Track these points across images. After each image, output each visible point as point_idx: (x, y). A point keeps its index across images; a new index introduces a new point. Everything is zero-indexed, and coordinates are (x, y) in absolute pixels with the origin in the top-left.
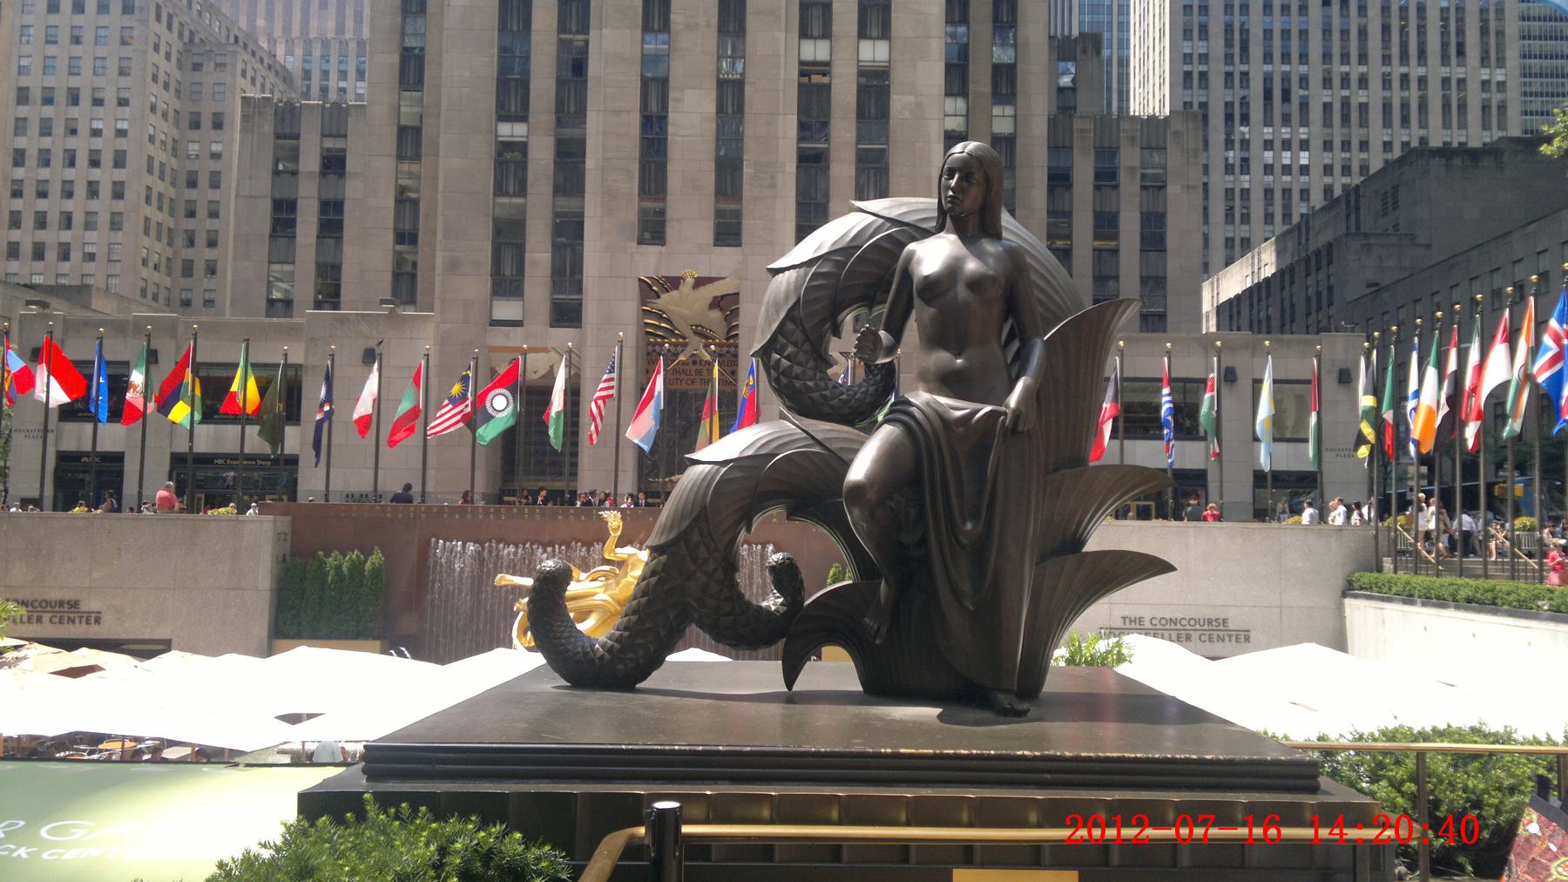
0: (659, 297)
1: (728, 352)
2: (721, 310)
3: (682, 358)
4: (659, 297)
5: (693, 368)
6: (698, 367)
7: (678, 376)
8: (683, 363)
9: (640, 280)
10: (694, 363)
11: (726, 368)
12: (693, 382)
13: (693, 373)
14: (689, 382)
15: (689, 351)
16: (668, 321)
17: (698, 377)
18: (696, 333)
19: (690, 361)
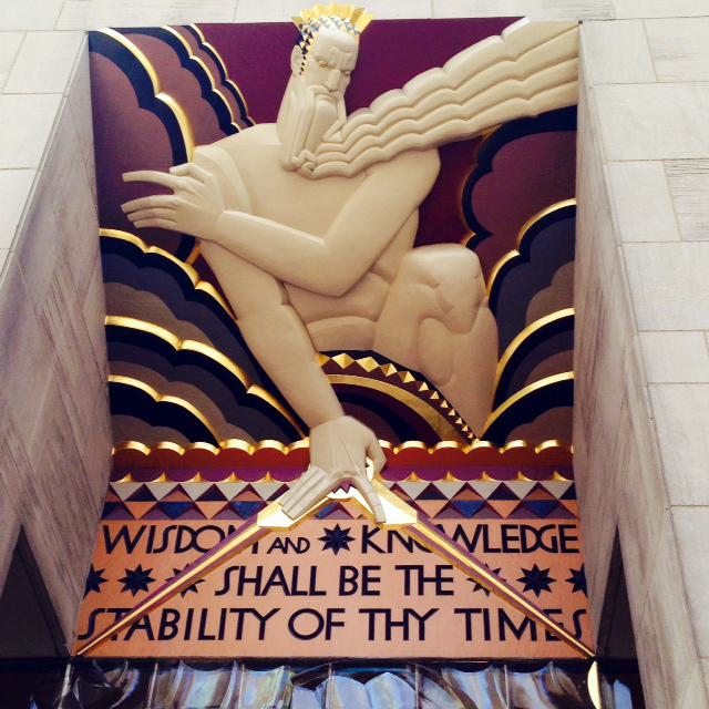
0: (180, 157)
1: (502, 493)
2: (483, 243)
3: (273, 517)
4: (180, 157)
5: (329, 564)
6: (353, 556)
7: (249, 599)
8: (282, 545)
9: (98, 44)
10: (336, 540)
11: (494, 560)
12: (327, 624)
13: (328, 580)
14: (307, 624)
15: (311, 486)
16: (222, 324)
17: (359, 600)
18: (355, 401)
19: (316, 530)
